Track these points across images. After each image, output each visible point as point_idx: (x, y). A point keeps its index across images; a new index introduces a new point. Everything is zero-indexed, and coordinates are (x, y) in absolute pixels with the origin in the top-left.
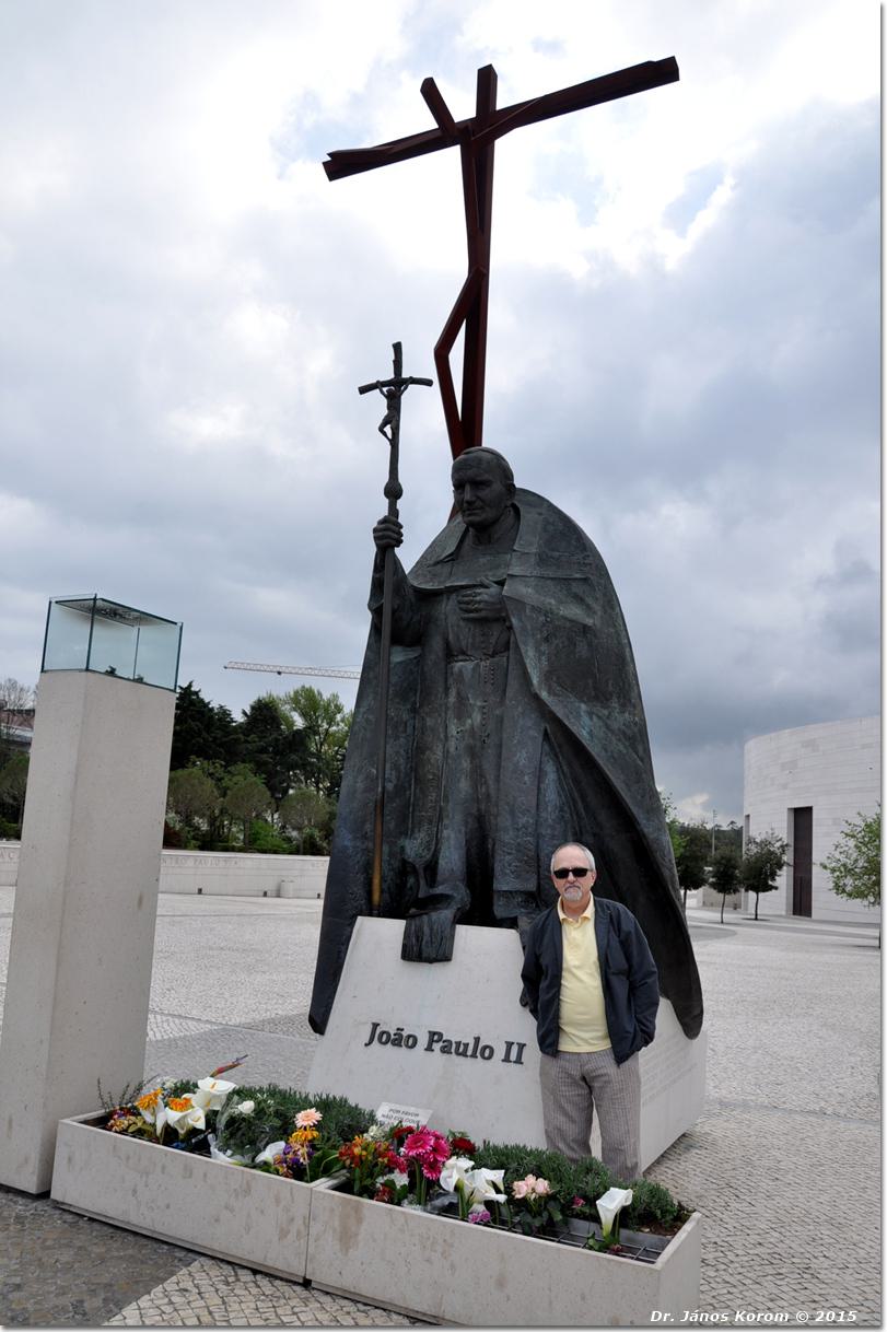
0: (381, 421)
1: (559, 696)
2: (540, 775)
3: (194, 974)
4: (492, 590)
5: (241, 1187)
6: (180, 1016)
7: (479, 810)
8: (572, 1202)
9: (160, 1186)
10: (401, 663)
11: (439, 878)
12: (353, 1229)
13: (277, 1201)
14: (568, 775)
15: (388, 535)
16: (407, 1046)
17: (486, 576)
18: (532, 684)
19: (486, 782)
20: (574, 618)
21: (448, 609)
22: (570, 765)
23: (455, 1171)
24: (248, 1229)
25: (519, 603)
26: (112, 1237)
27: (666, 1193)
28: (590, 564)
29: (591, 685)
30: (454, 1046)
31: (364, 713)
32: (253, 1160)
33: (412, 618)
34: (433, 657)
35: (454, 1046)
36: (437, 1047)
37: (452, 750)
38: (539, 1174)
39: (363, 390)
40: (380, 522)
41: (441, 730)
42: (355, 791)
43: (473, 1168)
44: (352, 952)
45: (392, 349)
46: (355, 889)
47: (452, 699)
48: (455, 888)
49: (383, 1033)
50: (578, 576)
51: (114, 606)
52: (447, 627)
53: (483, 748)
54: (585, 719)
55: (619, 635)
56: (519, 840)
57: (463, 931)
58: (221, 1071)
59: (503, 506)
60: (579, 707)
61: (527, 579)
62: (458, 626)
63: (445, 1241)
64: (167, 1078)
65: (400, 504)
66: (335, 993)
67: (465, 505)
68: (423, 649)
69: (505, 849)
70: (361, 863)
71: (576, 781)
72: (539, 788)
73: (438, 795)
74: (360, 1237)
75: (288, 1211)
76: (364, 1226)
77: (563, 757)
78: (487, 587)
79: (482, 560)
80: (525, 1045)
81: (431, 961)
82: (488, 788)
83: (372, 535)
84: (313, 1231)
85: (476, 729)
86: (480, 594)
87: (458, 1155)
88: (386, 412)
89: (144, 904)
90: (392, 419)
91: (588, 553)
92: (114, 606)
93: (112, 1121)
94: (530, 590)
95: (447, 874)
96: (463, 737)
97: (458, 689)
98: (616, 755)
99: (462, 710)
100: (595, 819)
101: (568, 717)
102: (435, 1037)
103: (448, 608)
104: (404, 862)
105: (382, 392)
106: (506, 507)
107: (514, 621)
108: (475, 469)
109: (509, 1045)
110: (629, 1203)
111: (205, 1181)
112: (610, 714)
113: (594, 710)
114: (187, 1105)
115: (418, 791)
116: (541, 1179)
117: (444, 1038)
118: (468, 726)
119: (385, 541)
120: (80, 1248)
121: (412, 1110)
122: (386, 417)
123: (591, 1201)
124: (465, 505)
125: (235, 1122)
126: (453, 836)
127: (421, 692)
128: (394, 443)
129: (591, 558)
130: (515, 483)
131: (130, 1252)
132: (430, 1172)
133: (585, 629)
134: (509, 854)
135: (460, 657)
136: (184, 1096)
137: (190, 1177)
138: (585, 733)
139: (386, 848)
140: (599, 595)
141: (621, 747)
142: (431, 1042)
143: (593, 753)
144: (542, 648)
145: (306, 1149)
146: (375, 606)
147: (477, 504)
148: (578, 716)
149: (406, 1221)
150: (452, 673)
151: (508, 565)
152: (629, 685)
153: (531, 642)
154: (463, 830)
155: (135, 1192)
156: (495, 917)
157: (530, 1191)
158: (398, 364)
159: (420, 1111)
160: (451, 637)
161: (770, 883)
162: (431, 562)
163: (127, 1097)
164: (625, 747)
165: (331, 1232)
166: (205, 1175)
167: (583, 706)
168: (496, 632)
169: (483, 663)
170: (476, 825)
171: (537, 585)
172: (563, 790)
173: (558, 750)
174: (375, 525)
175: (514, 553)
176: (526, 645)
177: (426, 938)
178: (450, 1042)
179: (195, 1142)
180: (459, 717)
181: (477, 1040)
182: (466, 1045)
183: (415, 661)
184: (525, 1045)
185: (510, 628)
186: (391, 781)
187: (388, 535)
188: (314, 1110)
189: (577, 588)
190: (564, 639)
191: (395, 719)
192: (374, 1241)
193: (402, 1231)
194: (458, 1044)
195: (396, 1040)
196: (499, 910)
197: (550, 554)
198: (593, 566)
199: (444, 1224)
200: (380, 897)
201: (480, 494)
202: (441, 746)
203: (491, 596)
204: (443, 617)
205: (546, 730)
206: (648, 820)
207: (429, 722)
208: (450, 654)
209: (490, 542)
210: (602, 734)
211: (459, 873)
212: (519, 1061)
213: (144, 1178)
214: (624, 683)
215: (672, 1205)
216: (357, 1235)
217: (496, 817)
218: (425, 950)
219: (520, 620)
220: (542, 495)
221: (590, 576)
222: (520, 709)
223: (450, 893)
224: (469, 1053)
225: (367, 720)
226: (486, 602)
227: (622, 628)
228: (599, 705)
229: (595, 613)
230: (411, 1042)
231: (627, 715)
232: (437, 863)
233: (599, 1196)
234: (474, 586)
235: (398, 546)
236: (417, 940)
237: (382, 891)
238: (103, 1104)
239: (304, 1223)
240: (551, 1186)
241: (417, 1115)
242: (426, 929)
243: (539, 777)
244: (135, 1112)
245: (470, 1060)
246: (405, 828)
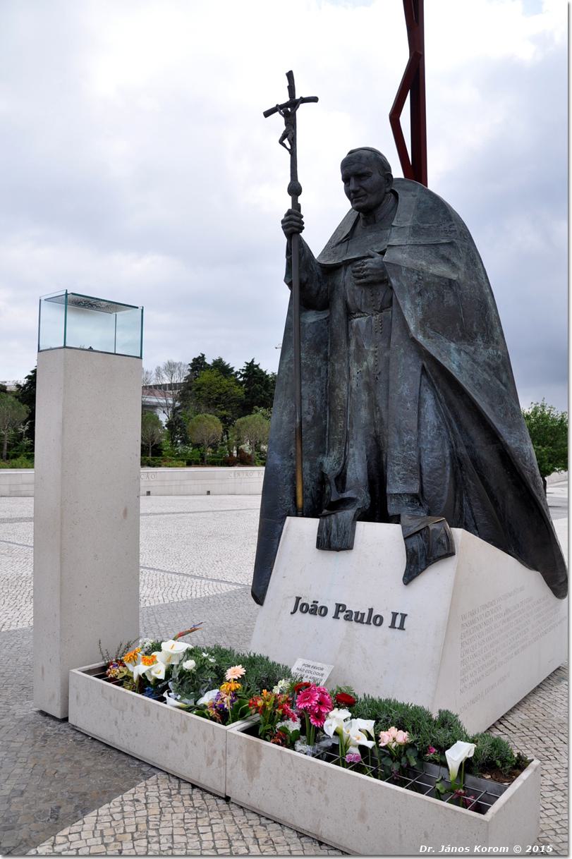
0: (280, 135)
1: (432, 338)
2: (420, 402)
3: (238, 550)
4: (376, 258)
5: (181, 725)
6: (218, 581)
7: (375, 431)
8: (426, 751)
10: (314, 323)
11: (348, 485)
12: (256, 763)
13: (205, 738)
14: (443, 400)
15: (293, 224)
16: (320, 615)
17: (372, 249)
18: (410, 331)
20: (442, 274)
21: (346, 280)
22: (444, 392)
23: (336, 720)
24: (187, 755)
25: (396, 266)
26: (102, 754)
27: (506, 745)
28: (455, 231)
29: (458, 328)
30: (354, 614)
31: (287, 363)
32: (195, 703)
33: (320, 288)
34: (337, 317)
35: (354, 614)
36: (342, 615)
37: (354, 387)
38: (401, 727)
39: (267, 114)
40: (286, 215)
41: (345, 372)
42: (282, 423)
43: (352, 718)
45: (286, 78)
46: (284, 496)
47: (353, 348)
48: (359, 492)
49: (303, 604)
50: (444, 241)
51: (86, 299)
52: (345, 292)
53: (376, 383)
54: (455, 355)
55: (482, 286)
57: (361, 525)
58: (181, 635)
59: (383, 192)
60: (449, 346)
61: (403, 247)
62: (353, 290)
63: (320, 779)
64: (148, 639)
65: (301, 199)
66: (271, 574)
67: (352, 194)
68: (330, 311)
69: (395, 461)
70: (288, 476)
71: (450, 405)
72: (419, 413)
73: (345, 422)
74: (261, 770)
75: (212, 745)
76: (263, 762)
77: (439, 387)
78: (373, 257)
79: (369, 237)
80: (406, 615)
81: (338, 550)
82: (381, 414)
83: (281, 225)
85: (370, 370)
86: (366, 263)
87: (339, 707)
88: (284, 128)
89: (129, 516)
90: (290, 135)
91: (454, 222)
92: (86, 299)
93: (109, 670)
94: (405, 256)
96: (361, 376)
97: (357, 339)
98: (480, 382)
99: (360, 358)
100: (468, 434)
101: (440, 354)
102: (340, 608)
103: (346, 277)
104: (323, 474)
105: (280, 113)
106: (386, 193)
107: (393, 281)
108: (356, 165)
109: (395, 615)
110: (471, 755)
111: (158, 720)
112: (476, 350)
113: (462, 347)
114: (153, 661)
115: (332, 420)
116: (401, 731)
117: (347, 610)
118: (364, 368)
119: (290, 229)
120: (77, 762)
121: (319, 665)
122: (285, 131)
123: (442, 749)
124: (352, 194)
125: (183, 673)
126: (357, 453)
127: (331, 344)
128: (293, 152)
129: (456, 226)
130: (393, 173)
131: (110, 766)
132: (316, 721)
133: (451, 283)
134: (397, 464)
136: (153, 654)
137: (149, 715)
138: (454, 366)
139: (307, 465)
140: (462, 254)
141: (486, 376)
142: (337, 612)
143: (461, 382)
145: (229, 698)
146: (288, 281)
147: (360, 193)
148: (449, 353)
149: (292, 760)
150: (352, 328)
151: (388, 238)
152: (492, 326)
153: (407, 297)
154: (364, 447)
155: (116, 722)
156: (388, 514)
157: (392, 740)
158: (291, 89)
159: (324, 666)
162: (334, 244)
163: (121, 652)
164: (489, 375)
165: (241, 763)
167: (453, 345)
168: (381, 292)
169: (374, 317)
170: (375, 443)
171: (410, 251)
172: (440, 413)
173: (434, 381)
174: (283, 217)
175: (393, 229)
176: (404, 300)
177: (334, 532)
178: (351, 612)
179: (151, 688)
180: (358, 361)
181: (371, 611)
182: (363, 615)
183: (325, 321)
184: (406, 615)
185: (391, 288)
186: (309, 414)
187: (293, 224)
188: (240, 666)
189: (444, 251)
191: (311, 366)
192: (271, 773)
193: (289, 768)
194: (357, 613)
195: (313, 609)
196: (392, 510)
197: (421, 225)
198: (458, 232)
199: (320, 766)
200: (303, 501)
201: (363, 184)
202: (346, 385)
203: (375, 263)
204: (341, 284)
205: (423, 366)
206: (510, 433)
207: (337, 366)
208: (349, 314)
209: (375, 222)
210: (469, 366)
211: (362, 481)
212: (401, 628)
214: (487, 325)
215: (512, 756)
216: (258, 768)
217: (387, 436)
219: (398, 280)
221: (454, 240)
222: (402, 351)
223: (354, 496)
224: (365, 621)
225: (289, 369)
226: (371, 269)
227: (484, 280)
228: (466, 343)
229: (459, 269)
230: (323, 611)
231: (490, 350)
232: (346, 474)
233: (448, 747)
234: (364, 258)
235: (301, 232)
236: (327, 534)
237: (305, 497)
238: (103, 658)
239: (223, 755)
240: (410, 737)
241: (322, 669)
242: (334, 526)
243: (419, 403)
244: (121, 663)
246: (322, 446)
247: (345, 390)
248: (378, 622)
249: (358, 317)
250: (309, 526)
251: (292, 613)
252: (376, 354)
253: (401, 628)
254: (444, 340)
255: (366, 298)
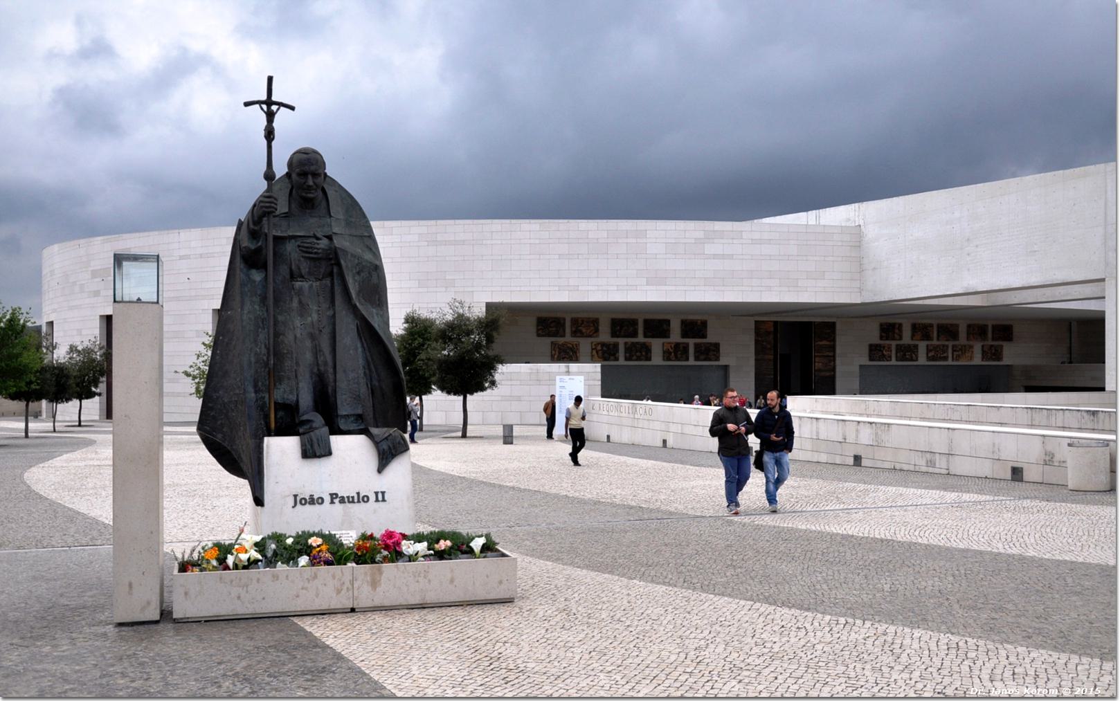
2: (356, 349)
7: (318, 370)
9: (257, 590)
16: (319, 504)
19: (323, 354)
24: (317, 595)
36: (336, 501)
37: (298, 335)
39: (247, 104)
42: (251, 363)
44: (267, 458)
56: (350, 387)
62: (299, 260)
78: (318, 239)
84: (356, 585)
95: (305, 409)
97: (300, 299)
99: (303, 309)
102: (333, 496)
105: (262, 109)
109: (376, 493)
117: (340, 495)
134: (345, 394)
135: (299, 279)
144: (356, 278)
155: (239, 598)
159: (349, 532)
160: (293, 267)
161: (93, 389)
166: (287, 576)
167: (374, 310)
178: (343, 497)
180: (302, 316)
181: (358, 494)
182: (353, 497)
190: (367, 273)
194: (348, 497)
201: (316, 181)
213: (245, 588)
216: (380, 580)
218: (314, 451)
219: (345, 262)
220: (334, 178)
223: (312, 418)
224: (356, 501)
225: (250, 319)
242: (315, 440)
245: (357, 505)
247: (291, 337)
248: (366, 499)
249: (300, 281)
250: (290, 444)
251: (293, 507)
252: (320, 312)
253: (384, 500)
254: (370, 306)
255: (310, 268)
